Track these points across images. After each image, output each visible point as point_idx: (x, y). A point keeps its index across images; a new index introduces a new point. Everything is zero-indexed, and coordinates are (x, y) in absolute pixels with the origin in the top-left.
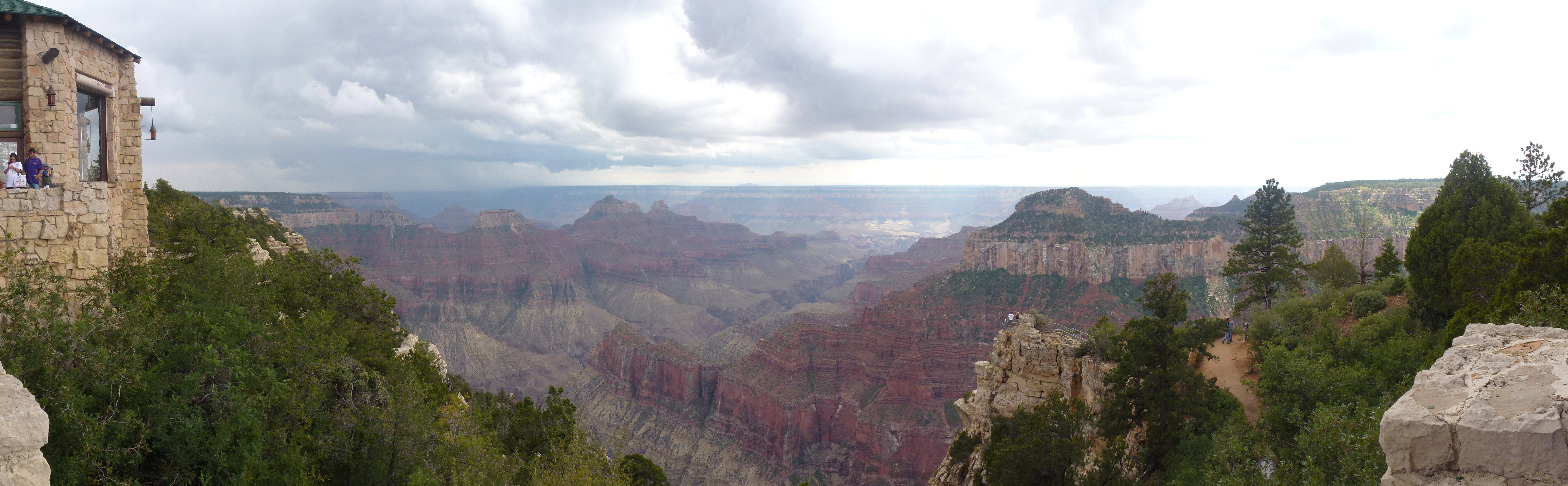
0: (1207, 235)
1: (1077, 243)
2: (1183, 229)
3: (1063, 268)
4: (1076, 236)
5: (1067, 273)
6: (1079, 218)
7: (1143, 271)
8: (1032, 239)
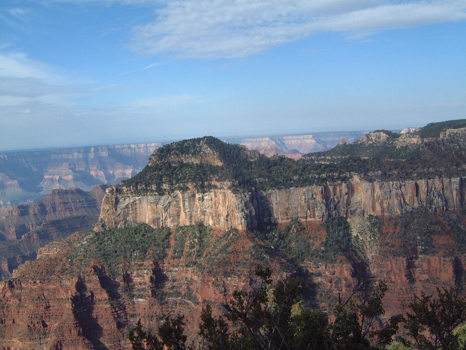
0: (346, 177)
1: (219, 191)
2: (324, 172)
3: (206, 217)
4: (218, 184)
5: (211, 222)
6: (218, 166)
7: (287, 214)
8: (173, 191)
